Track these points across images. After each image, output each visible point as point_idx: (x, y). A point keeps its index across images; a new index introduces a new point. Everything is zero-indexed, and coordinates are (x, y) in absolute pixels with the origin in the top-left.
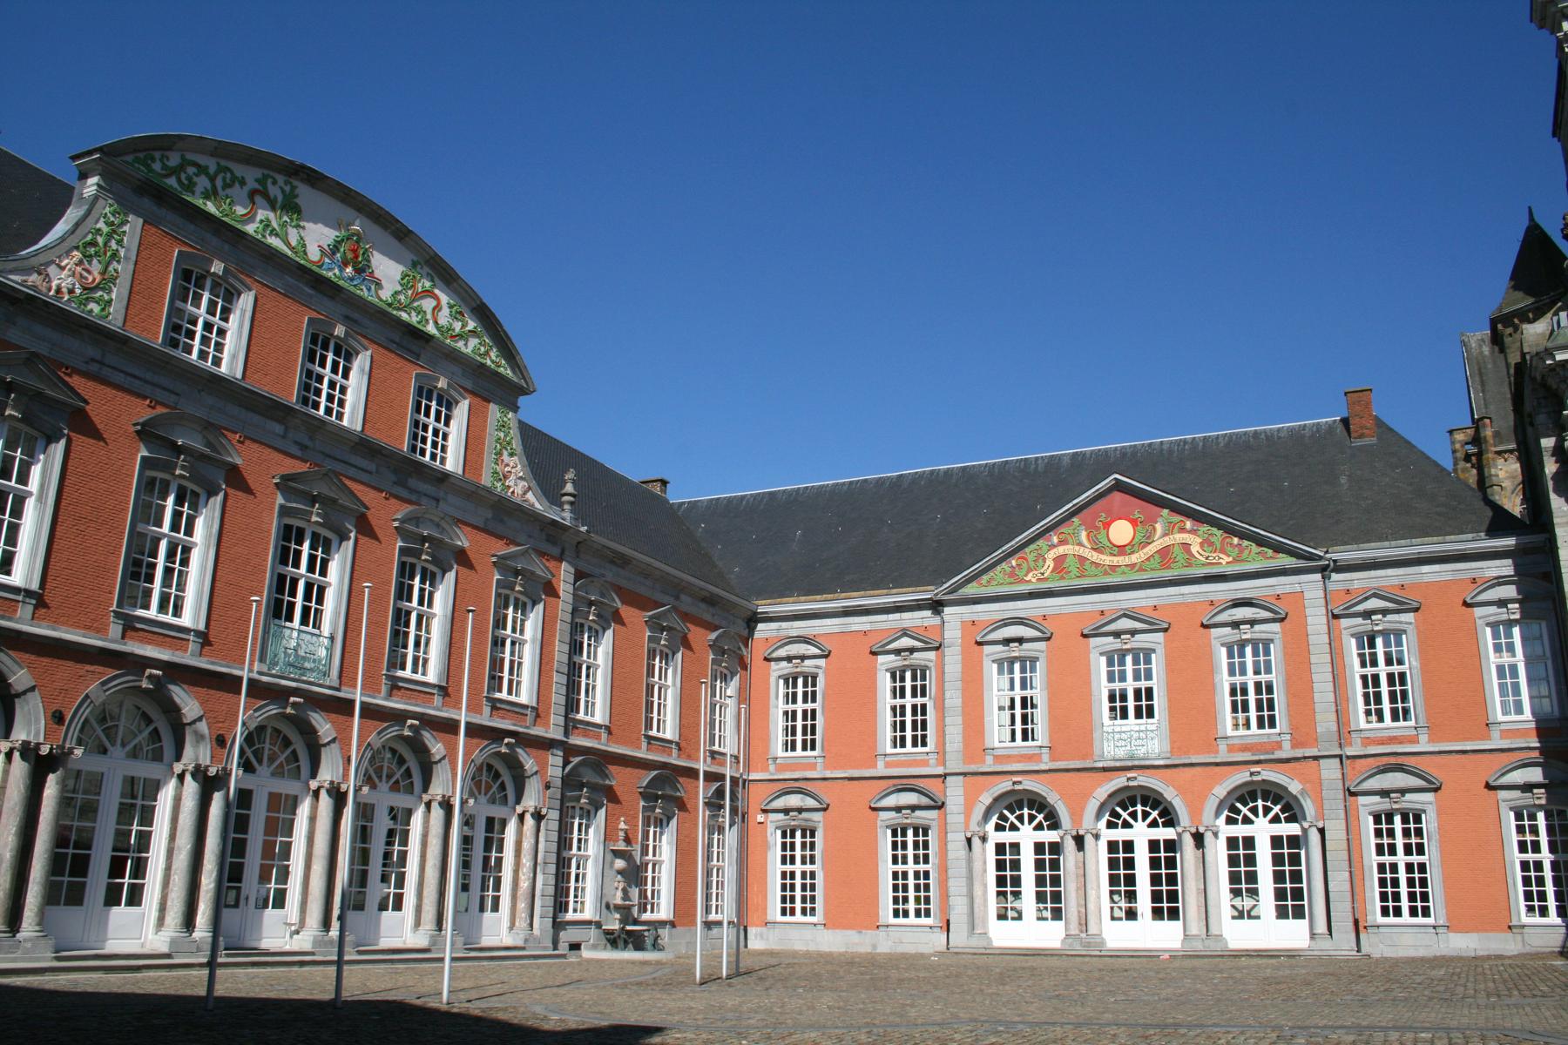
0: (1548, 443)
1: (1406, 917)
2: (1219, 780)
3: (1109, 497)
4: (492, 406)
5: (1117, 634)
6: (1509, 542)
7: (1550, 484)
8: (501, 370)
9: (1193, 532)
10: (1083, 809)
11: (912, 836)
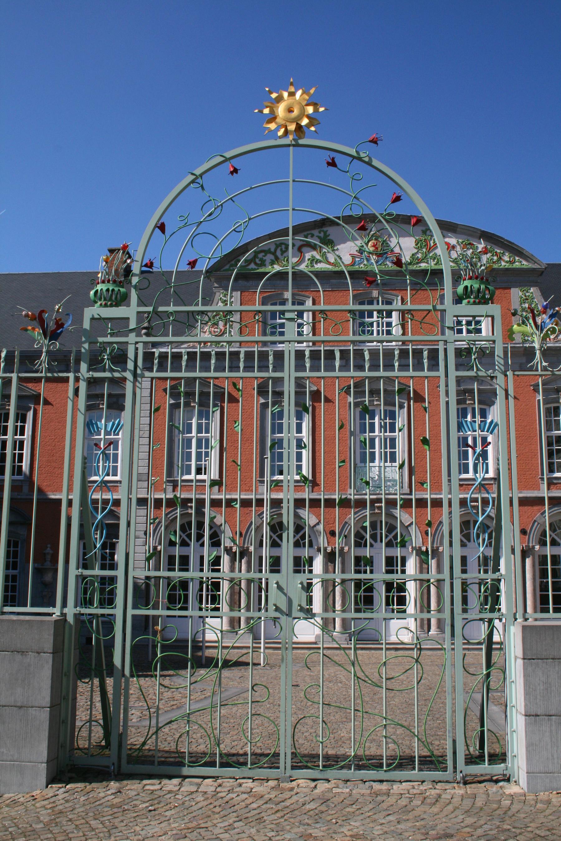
4: (513, 290)
8: (517, 265)
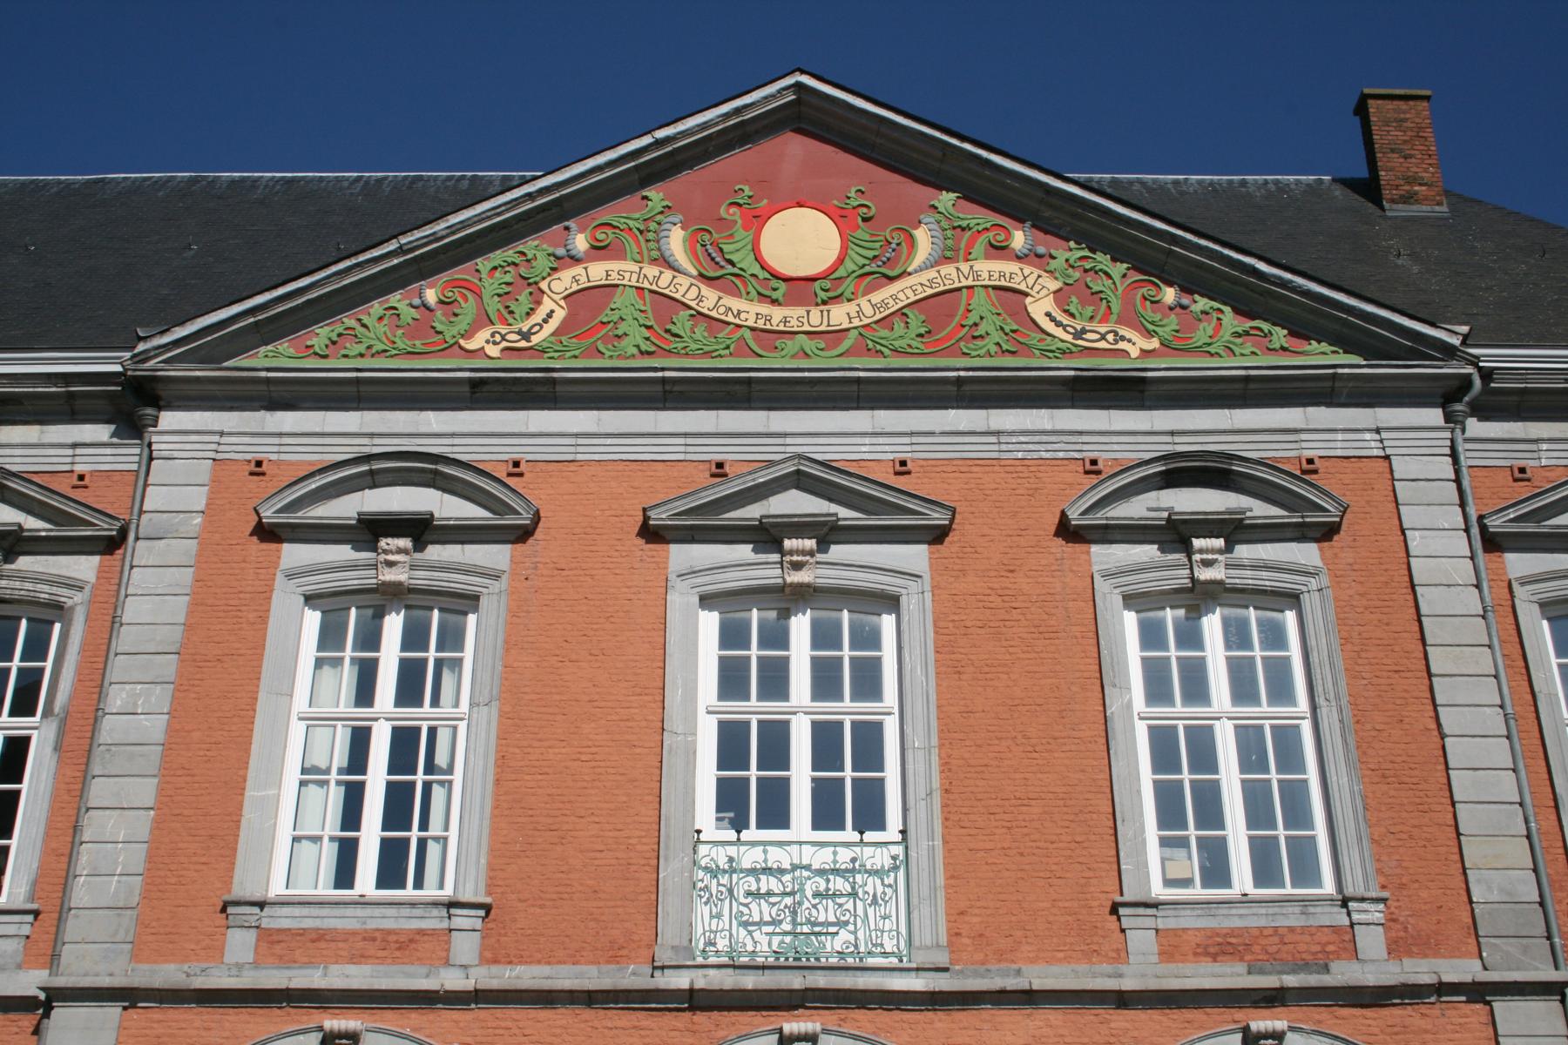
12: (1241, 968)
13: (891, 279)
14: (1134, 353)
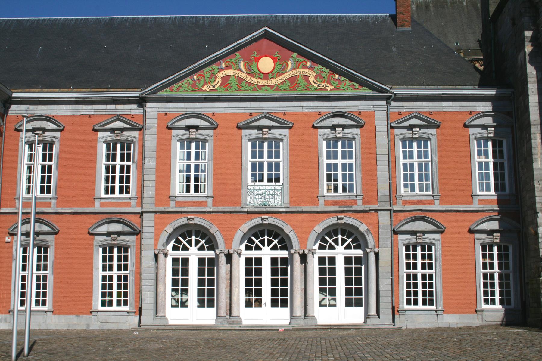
0: (528, 34)
1: (420, 306)
2: (318, 222)
3: (260, 42)
5: (260, 128)
6: (493, 92)
7: (528, 58)
9: (311, 68)
10: (232, 237)
11: (117, 252)
12: (338, 207)
13: (284, 73)
14: (329, 89)
